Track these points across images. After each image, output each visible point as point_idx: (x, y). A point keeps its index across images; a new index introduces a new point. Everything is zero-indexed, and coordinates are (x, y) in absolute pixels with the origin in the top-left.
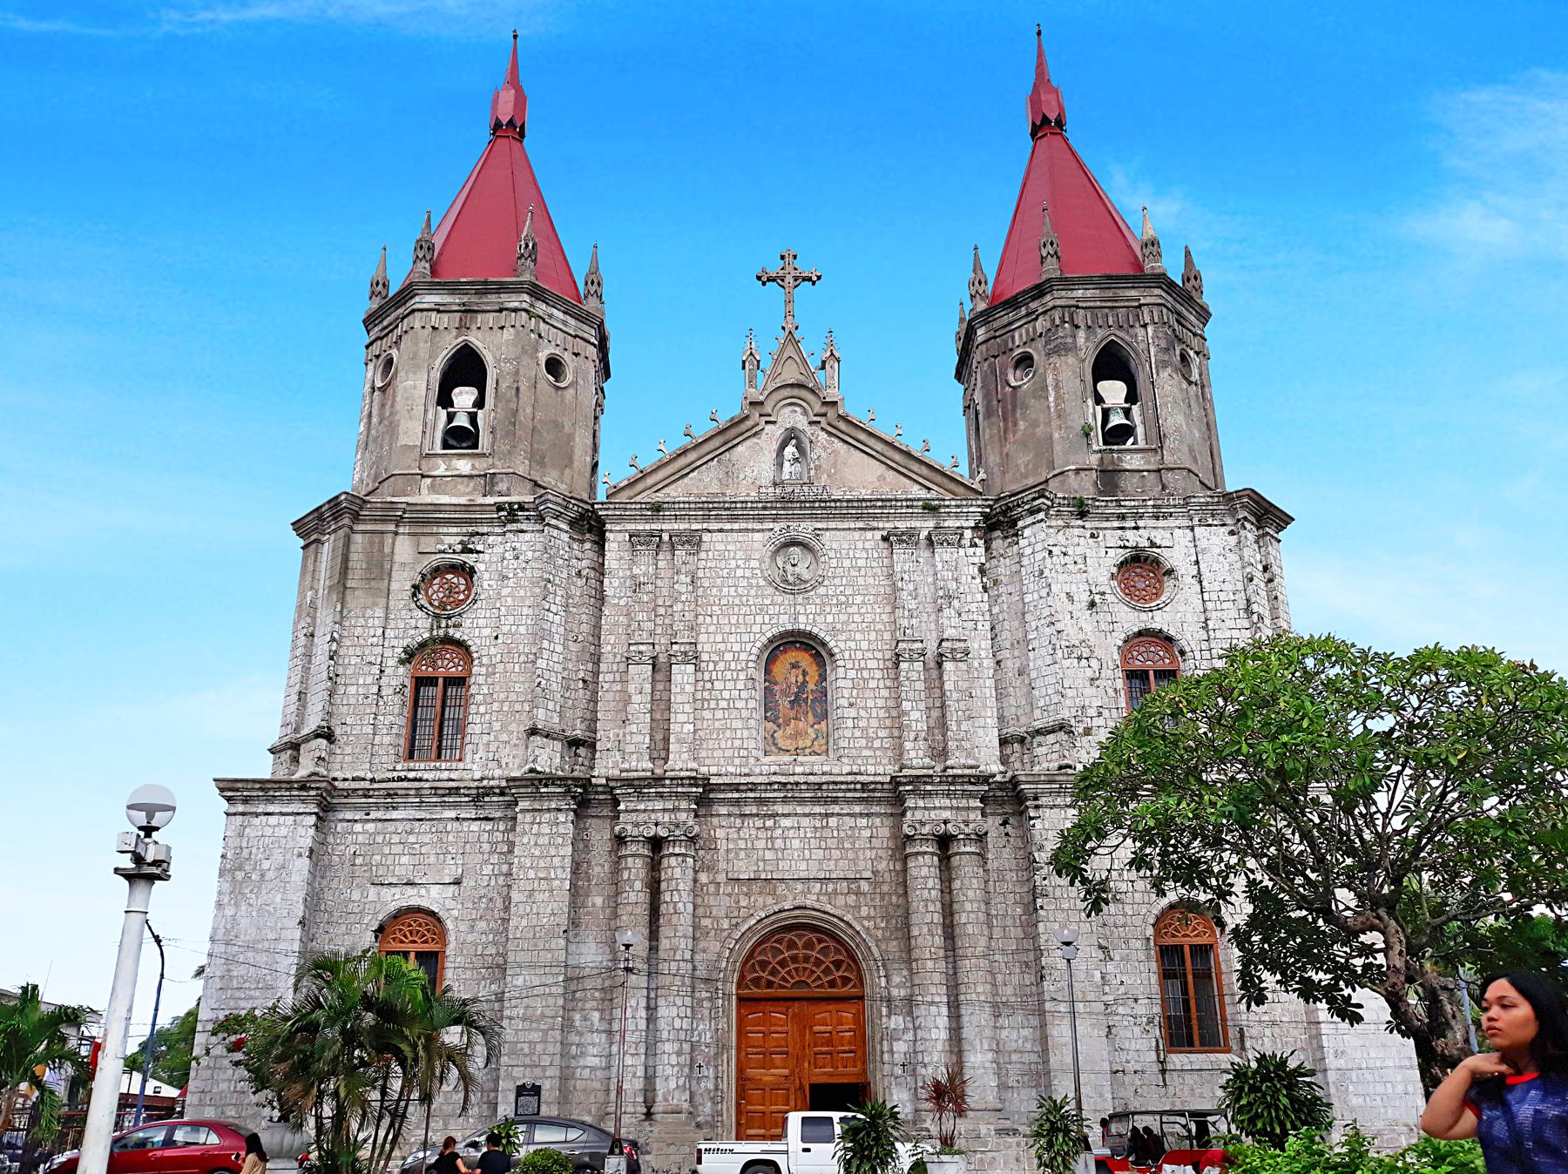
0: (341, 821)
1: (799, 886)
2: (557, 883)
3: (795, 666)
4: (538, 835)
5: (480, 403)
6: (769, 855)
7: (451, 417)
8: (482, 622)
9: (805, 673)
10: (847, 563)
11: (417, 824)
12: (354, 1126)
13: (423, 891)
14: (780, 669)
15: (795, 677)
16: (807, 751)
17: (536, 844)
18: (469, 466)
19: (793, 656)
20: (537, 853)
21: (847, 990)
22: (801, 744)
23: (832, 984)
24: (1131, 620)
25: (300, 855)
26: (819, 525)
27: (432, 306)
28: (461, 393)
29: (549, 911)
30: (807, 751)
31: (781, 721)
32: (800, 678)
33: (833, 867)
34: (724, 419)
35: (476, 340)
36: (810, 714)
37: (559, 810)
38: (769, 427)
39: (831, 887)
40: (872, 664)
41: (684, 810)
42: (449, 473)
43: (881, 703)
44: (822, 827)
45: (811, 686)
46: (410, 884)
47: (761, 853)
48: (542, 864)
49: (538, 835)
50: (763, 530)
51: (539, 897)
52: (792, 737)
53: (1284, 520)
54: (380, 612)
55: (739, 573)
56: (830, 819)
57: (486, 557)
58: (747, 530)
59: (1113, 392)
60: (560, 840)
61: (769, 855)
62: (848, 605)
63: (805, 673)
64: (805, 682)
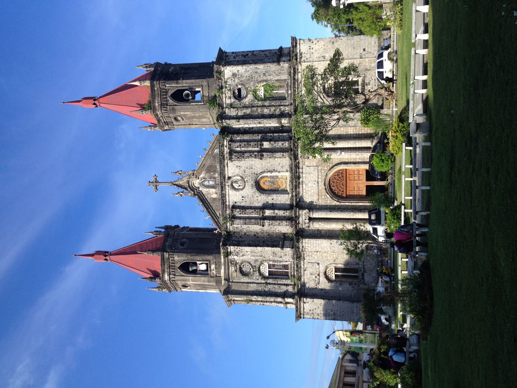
0: (304, 292)
1: (320, 184)
2: (319, 242)
3: (264, 183)
4: (308, 247)
6: (312, 191)
11: (305, 274)
12: (411, 316)
13: (321, 272)
14: (265, 187)
15: (267, 184)
16: (286, 180)
17: (310, 247)
18: (213, 265)
19: (262, 184)
20: (312, 247)
21: (344, 173)
22: (284, 182)
23: (343, 176)
25: (313, 301)
26: (227, 178)
27: (168, 276)
29: (326, 244)
30: (286, 180)
31: (278, 187)
32: (268, 182)
33: (315, 176)
35: (178, 265)
36: (277, 180)
37: (302, 242)
38: (200, 189)
39: (320, 176)
41: (302, 212)
42: (215, 270)
44: (305, 178)
45: (269, 179)
46: (319, 275)
47: (312, 193)
48: (315, 246)
49: (308, 247)
50: (229, 192)
51: (323, 246)
52: (282, 184)
53: (220, 50)
56: (303, 176)
58: (229, 194)
60: (309, 242)
61: (312, 191)
63: (266, 181)
64: (269, 181)
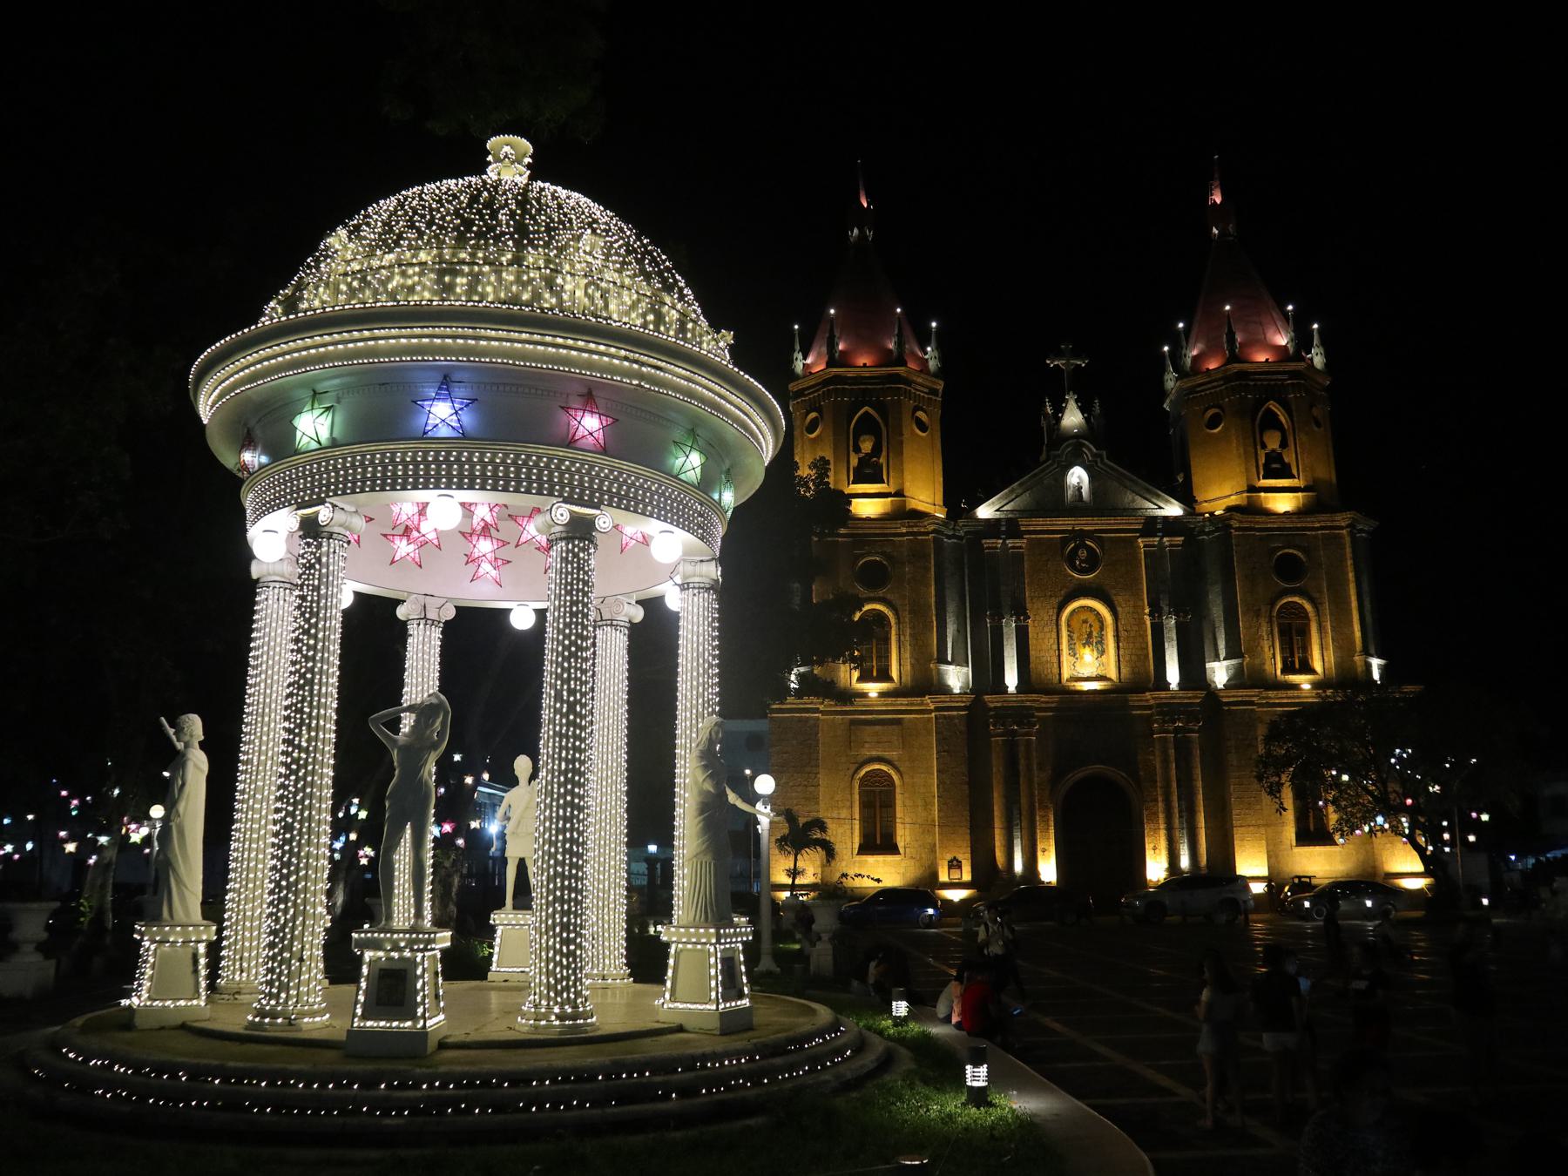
3: (1085, 622)
5: (877, 450)
9: (1091, 626)
28: (864, 441)
63: (1091, 626)
64: (1091, 632)
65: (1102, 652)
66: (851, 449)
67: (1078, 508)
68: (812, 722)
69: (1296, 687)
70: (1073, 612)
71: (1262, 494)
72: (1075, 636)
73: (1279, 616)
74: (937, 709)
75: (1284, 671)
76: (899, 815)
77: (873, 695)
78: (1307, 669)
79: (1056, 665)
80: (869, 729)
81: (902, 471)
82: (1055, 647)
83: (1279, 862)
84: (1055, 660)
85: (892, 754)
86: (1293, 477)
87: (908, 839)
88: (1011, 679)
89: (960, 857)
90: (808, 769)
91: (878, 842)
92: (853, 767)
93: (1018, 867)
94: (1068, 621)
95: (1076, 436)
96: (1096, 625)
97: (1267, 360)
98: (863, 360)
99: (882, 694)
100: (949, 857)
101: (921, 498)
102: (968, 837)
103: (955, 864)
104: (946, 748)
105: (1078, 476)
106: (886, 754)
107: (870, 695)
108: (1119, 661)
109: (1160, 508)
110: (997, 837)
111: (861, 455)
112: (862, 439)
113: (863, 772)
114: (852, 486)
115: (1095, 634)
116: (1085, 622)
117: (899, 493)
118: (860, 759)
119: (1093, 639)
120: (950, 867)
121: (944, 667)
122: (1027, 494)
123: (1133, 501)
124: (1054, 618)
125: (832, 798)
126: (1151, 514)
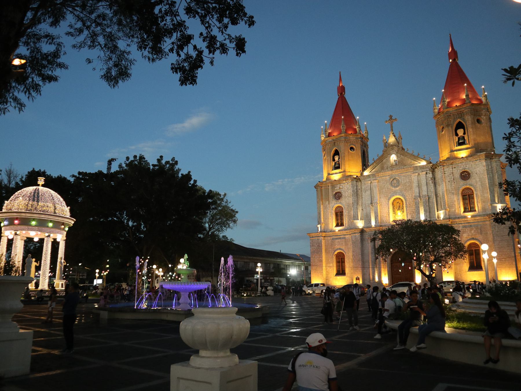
3: (398, 203)
7: (335, 163)
8: (344, 201)
9: (400, 204)
10: (405, 181)
24: (463, 185)
34: (380, 155)
40: (411, 201)
43: (413, 208)
54: (328, 202)
55: (386, 186)
57: (343, 189)
59: (460, 132)
62: (406, 190)
64: (400, 206)
65: (403, 212)
66: (332, 160)
67: (392, 167)
68: (320, 240)
69: (465, 217)
70: (394, 200)
71: (455, 152)
72: (395, 207)
73: (462, 193)
74: (352, 234)
75: (464, 212)
76: (346, 265)
77: (337, 231)
78: (472, 210)
79: (388, 217)
80: (337, 240)
81: (345, 165)
82: (388, 212)
83: (461, 277)
84: (388, 215)
85: (343, 248)
86: (467, 144)
87: (348, 271)
88: (373, 223)
89: (359, 277)
90: (319, 253)
91: (341, 272)
92: (333, 251)
93: (377, 279)
94: (393, 203)
95: (392, 146)
96: (401, 203)
97: (456, 105)
98: (335, 134)
99: (339, 231)
100: (356, 277)
101: (353, 171)
102: (361, 271)
103: (358, 279)
104: (354, 245)
105: (393, 158)
106: (342, 248)
107: (336, 231)
108: (407, 214)
109: (420, 163)
110: (371, 270)
111: (335, 162)
112: (335, 157)
113: (336, 253)
114: (332, 171)
115: (401, 206)
116: (398, 203)
117: (344, 171)
118: (335, 249)
119: (401, 208)
120: (356, 279)
121: (355, 221)
122: (379, 165)
123: (411, 162)
124: (387, 203)
125: (328, 261)
126: (415, 166)
